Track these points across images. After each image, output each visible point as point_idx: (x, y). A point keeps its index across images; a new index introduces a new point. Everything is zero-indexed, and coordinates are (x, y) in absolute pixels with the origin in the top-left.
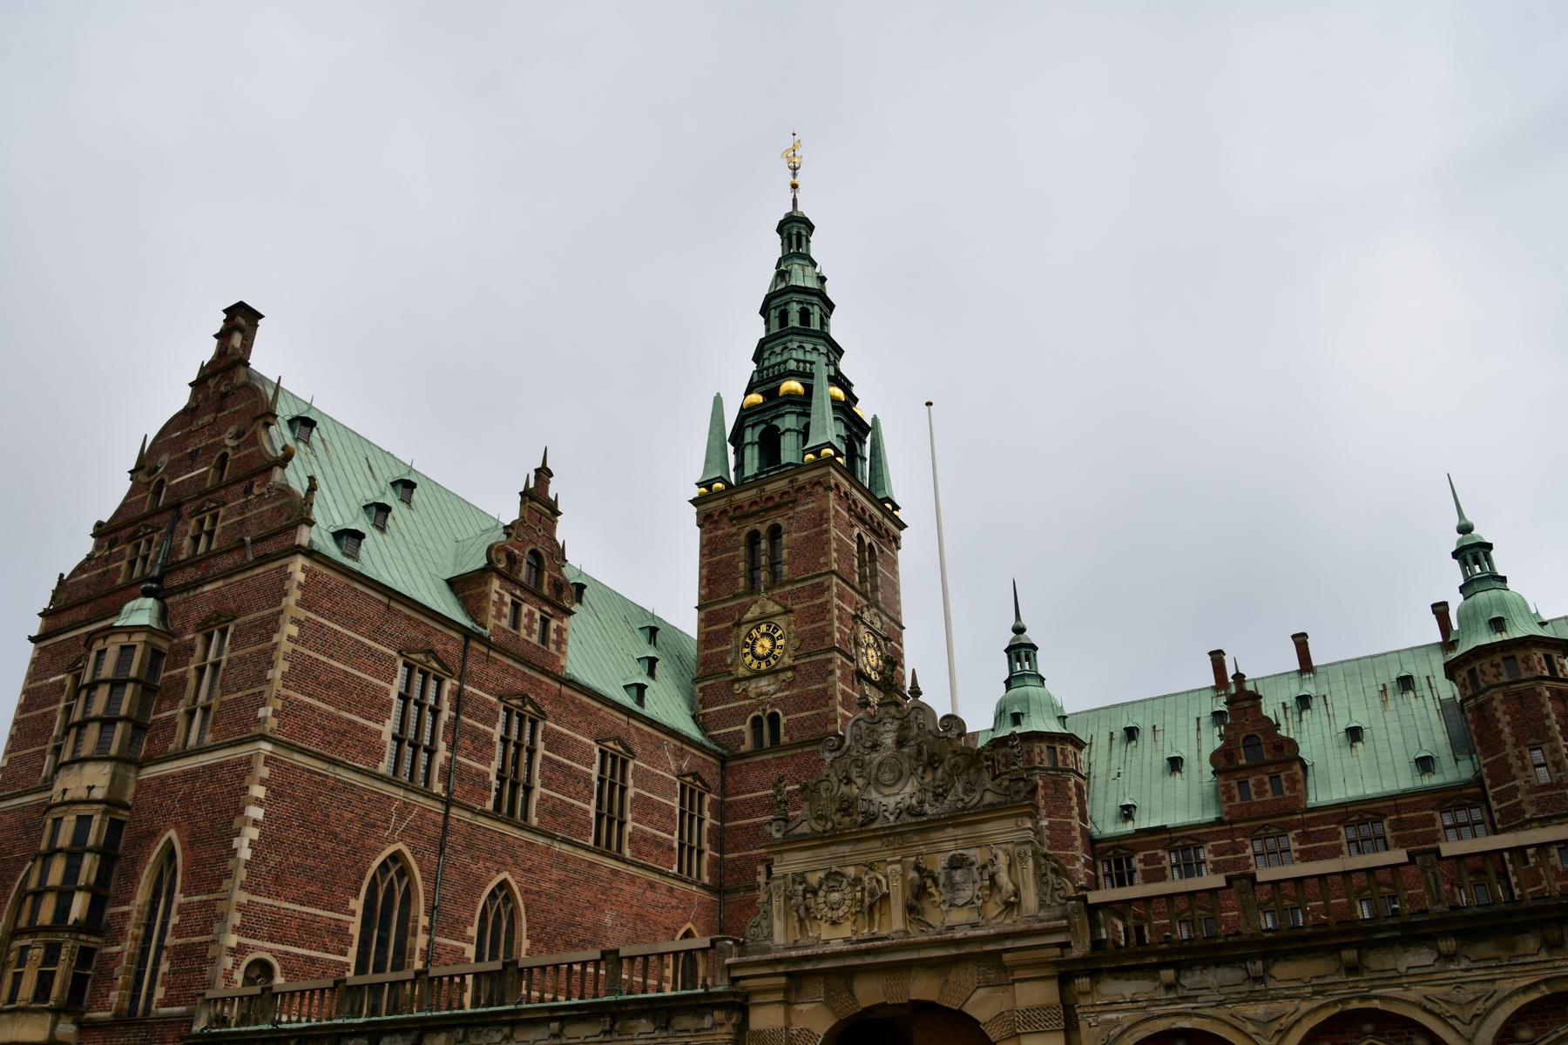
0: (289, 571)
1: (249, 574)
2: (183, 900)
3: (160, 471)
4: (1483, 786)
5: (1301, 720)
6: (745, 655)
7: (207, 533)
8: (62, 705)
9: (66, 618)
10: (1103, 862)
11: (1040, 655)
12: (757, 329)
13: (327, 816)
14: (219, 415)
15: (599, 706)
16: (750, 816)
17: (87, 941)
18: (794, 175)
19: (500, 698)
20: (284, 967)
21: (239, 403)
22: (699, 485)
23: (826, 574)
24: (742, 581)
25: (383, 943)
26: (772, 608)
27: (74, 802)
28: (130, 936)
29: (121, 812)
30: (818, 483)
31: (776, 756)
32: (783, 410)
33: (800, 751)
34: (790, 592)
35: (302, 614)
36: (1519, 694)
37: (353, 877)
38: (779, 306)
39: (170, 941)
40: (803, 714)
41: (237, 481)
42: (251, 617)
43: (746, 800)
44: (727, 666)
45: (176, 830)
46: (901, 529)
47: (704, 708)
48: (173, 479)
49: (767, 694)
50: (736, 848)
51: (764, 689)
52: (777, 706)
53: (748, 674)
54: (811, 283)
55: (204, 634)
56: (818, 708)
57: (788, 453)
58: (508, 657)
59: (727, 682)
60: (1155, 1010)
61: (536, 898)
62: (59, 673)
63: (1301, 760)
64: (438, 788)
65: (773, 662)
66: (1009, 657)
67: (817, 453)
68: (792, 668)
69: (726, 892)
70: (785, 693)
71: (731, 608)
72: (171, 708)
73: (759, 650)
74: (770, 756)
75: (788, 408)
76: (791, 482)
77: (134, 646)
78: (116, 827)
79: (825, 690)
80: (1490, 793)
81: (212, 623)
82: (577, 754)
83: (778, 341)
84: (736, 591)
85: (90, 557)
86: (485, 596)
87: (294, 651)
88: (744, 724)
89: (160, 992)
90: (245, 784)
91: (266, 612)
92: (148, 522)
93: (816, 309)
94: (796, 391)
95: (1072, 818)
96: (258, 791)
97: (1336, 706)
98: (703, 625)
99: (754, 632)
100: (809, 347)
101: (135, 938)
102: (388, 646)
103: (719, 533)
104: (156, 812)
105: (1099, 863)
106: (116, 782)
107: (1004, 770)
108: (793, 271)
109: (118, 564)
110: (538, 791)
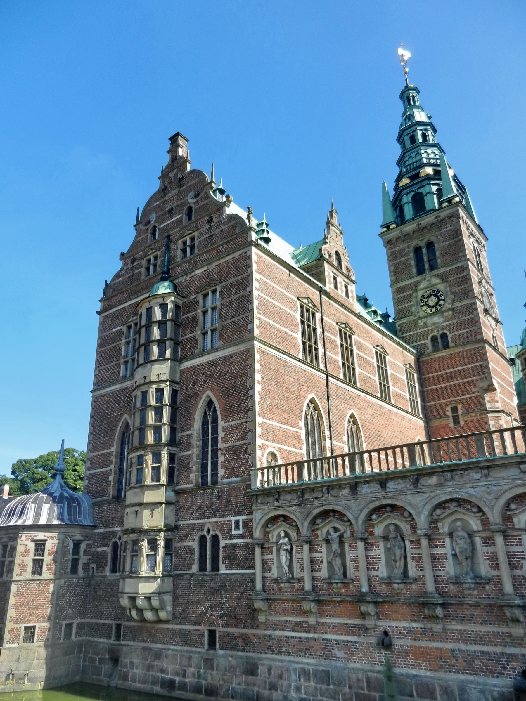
0: (248, 255)
2: (224, 425)
6: (422, 306)
7: (189, 246)
8: (124, 341)
9: (115, 300)
12: (397, 150)
13: (284, 379)
14: (181, 189)
16: (438, 384)
17: (172, 450)
19: (337, 323)
22: (382, 226)
25: (314, 443)
28: (195, 444)
29: (176, 385)
30: (453, 216)
32: (423, 183)
37: (299, 410)
38: (409, 133)
39: (220, 445)
42: (230, 281)
43: (434, 376)
45: (211, 391)
47: (402, 334)
48: (161, 224)
50: (432, 400)
53: (425, 314)
55: (202, 295)
56: (470, 327)
58: (337, 303)
61: (364, 422)
62: (118, 326)
64: (322, 367)
65: (439, 308)
68: (453, 310)
70: (449, 323)
71: (410, 284)
72: (192, 332)
73: (430, 303)
78: (174, 393)
79: (473, 319)
82: (368, 353)
83: (412, 151)
85: (121, 270)
86: (323, 272)
87: (259, 295)
89: (221, 472)
91: (239, 277)
98: (395, 294)
101: (198, 446)
103: (397, 248)
104: (196, 384)
106: (172, 371)
109: (139, 270)
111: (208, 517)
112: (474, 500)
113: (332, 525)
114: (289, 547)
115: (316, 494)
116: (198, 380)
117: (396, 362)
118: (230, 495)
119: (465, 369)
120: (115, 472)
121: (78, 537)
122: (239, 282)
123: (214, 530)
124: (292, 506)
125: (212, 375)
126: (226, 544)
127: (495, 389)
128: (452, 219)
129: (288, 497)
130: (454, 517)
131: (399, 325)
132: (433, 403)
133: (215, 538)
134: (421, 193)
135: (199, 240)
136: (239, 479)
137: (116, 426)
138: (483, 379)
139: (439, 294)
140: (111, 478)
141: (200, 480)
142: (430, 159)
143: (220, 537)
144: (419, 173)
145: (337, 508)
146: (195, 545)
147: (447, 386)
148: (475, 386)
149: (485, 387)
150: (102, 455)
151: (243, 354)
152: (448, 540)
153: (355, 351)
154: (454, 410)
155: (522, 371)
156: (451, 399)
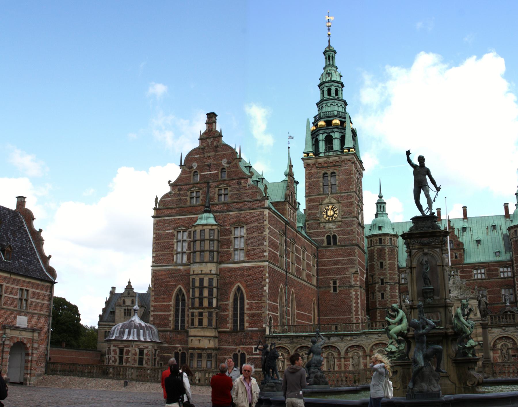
1: (247, 211)
3: (195, 168)
4: (512, 262)
5: (463, 235)
9: (166, 212)
15: (301, 237)
21: (224, 151)
22: (304, 153)
23: (352, 192)
24: (322, 189)
27: (206, 274)
28: (230, 310)
31: (336, 248)
33: (344, 248)
34: (339, 196)
35: (269, 226)
39: (246, 311)
41: (234, 180)
42: (253, 225)
44: (317, 217)
47: (309, 230)
49: (332, 228)
51: (331, 227)
52: (336, 233)
53: (325, 221)
54: (338, 79)
56: (350, 235)
57: (336, 146)
59: (317, 223)
60: (501, 333)
62: (170, 230)
63: (464, 249)
65: (334, 218)
67: (349, 150)
68: (341, 221)
69: (320, 288)
72: (227, 248)
73: (329, 213)
74: (333, 248)
75: (335, 130)
76: (339, 158)
77: (214, 230)
79: (352, 230)
80: (515, 265)
81: (237, 224)
83: (329, 101)
84: (320, 193)
86: (286, 209)
88: (324, 237)
89: (246, 324)
92: (195, 185)
93: (340, 88)
94: (338, 124)
96: (267, 275)
97: (474, 232)
98: (308, 202)
99: (327, 207)
101: (232, 311)
103: (312, 171)
105: (400, 275)
107: (375, 244)
108: (333, 73)
109: (185, 197)
110: (296, 264)
111: (239, 345)
113: (304, 352)
114: (283, 360)
115: (299, 339)
116: (232, 276)
118: (252, 336)
119: (344, 259)
120: (173, 316)
121: (156, 348)
122: (258, 228)
124: (287, 343)
125: (240, 275)
126: (250, 357)
128: (349, 162)
129: (285, 339)
130: (356, 351)
131: (308, 224)
134: (332, 137)
136: (257, 329)
137: (173, 290)
138: (353, 267)
139: (335, 210)
140: (171, 319)
141: (233, 327)
142: (339, 112)
143: (246, 354)
144: (332, 120)
148: (348, 271)
149: (353, 272)
150: (162, 305)
152: (351, 359)
153: (295, 254)
154: (335, 283)
155: (367, 248)
156: (333, 276)
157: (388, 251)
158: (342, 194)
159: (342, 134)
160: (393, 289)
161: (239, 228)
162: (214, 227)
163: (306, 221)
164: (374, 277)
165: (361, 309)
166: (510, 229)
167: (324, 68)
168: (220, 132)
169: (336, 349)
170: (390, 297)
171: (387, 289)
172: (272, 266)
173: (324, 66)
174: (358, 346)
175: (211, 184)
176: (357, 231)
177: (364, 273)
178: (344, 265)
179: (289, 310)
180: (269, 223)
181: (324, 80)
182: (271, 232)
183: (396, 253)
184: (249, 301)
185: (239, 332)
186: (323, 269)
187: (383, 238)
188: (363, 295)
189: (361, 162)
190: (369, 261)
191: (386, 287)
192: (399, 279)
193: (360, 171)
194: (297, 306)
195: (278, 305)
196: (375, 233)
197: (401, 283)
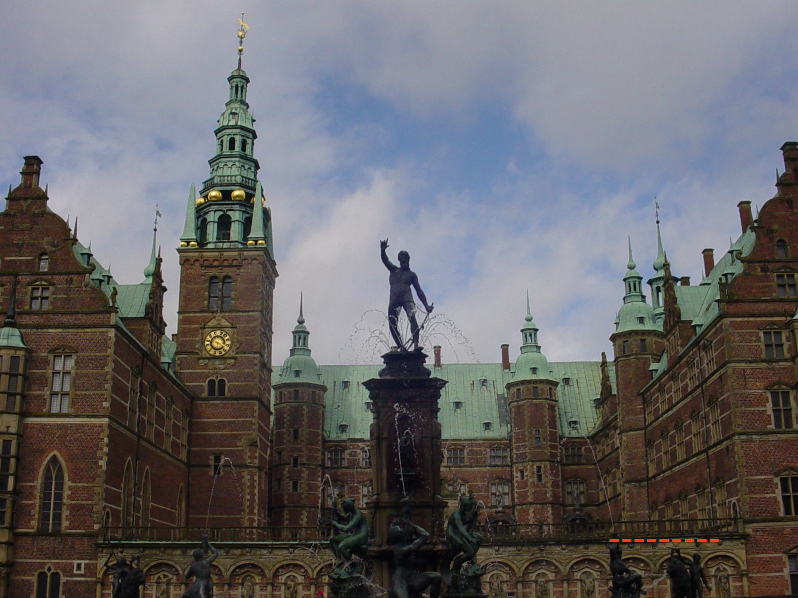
1: (80, 330)
4: (510, 440)
10: (328, 452)
11: (310, 338)
18: (241, 42)
20: (112, 514)
24: (206, 302)
26: (225, 323)
30: (256, 259)
31: (224, 402)
33: (236, 402)
36: (536, 405)
39: (65, 501)
40: (238, 383)
41: (60, 274)
44: (196, 349)
46: (276, 277)
47: (181, 369)
52: (224, 376)
53: (208, 356)
54: (248, 125)
66: (295, 337)
68: (235, 358)
69: (192, 466)
72: (39, 390)
73: (215, 345)
74: (219, 402)
75: (237, 207)
77: (19, 357)
80: (514, 446)
81: (60, 351)
89: (65, 523)
90: (101, 437)
91: (98, 354)
95: (319, 429)
96: (106, 440)
100: (247, 167)
102: (128, 366)
104: (42, 441)
105: (326, 452)
110: (155, 425)
112: (260, 565)
113: (163, 573)
116: (44, 438)
117: (178, 410)
119: (234, 421)
123: (55, 569)
126: (67, 580)
127: (257, 446)
131: (179, 359)
132: (197, 449)
133: (55, 576)
134: (231, 218)
135: (55, 296)
136: (84, 531)
139: (226, 338)
143: (62, 575)
144: (232, 191)
145: (170, 562)
146: (34, 579)
147: (215, 434)
151: (96, 427)
153: (156, 407)
156: (216, 448)
157: (308, 413)
158: (238, 314)
159: (248, 215)
160: (312, 475)
161: (63, 357)
162: (21, 353)
163: (177, 353)
164: (283, 453)
165: (259, 505)
166: (509, 386)
167: (227, 105)
168: (44, 190)
169: (217, 570)
170: (307, 488)
171: (303, 475)
172: (115, 425)
173: (228, 100)
174: (254, 566)
175: (20, 277)
176: (260, 376)
177: (267, 445)
178: (235, 431)
179: (139, 501)
180: (115, 353)
181: (226, 124)
182: (118, 368)
183: (321, 416)
184: (72, 483)
185: (51, 535)
186: (199, 435)
187: (301, 390)
188: (263, 482)
189: (273, 263)
190: (275, 427)
191: (301, 472)
192: (323, 460)
193: (272, 277)
194: (153, 495)
195: (122, 491)
196: (288, 382)
197: (326, 465)
